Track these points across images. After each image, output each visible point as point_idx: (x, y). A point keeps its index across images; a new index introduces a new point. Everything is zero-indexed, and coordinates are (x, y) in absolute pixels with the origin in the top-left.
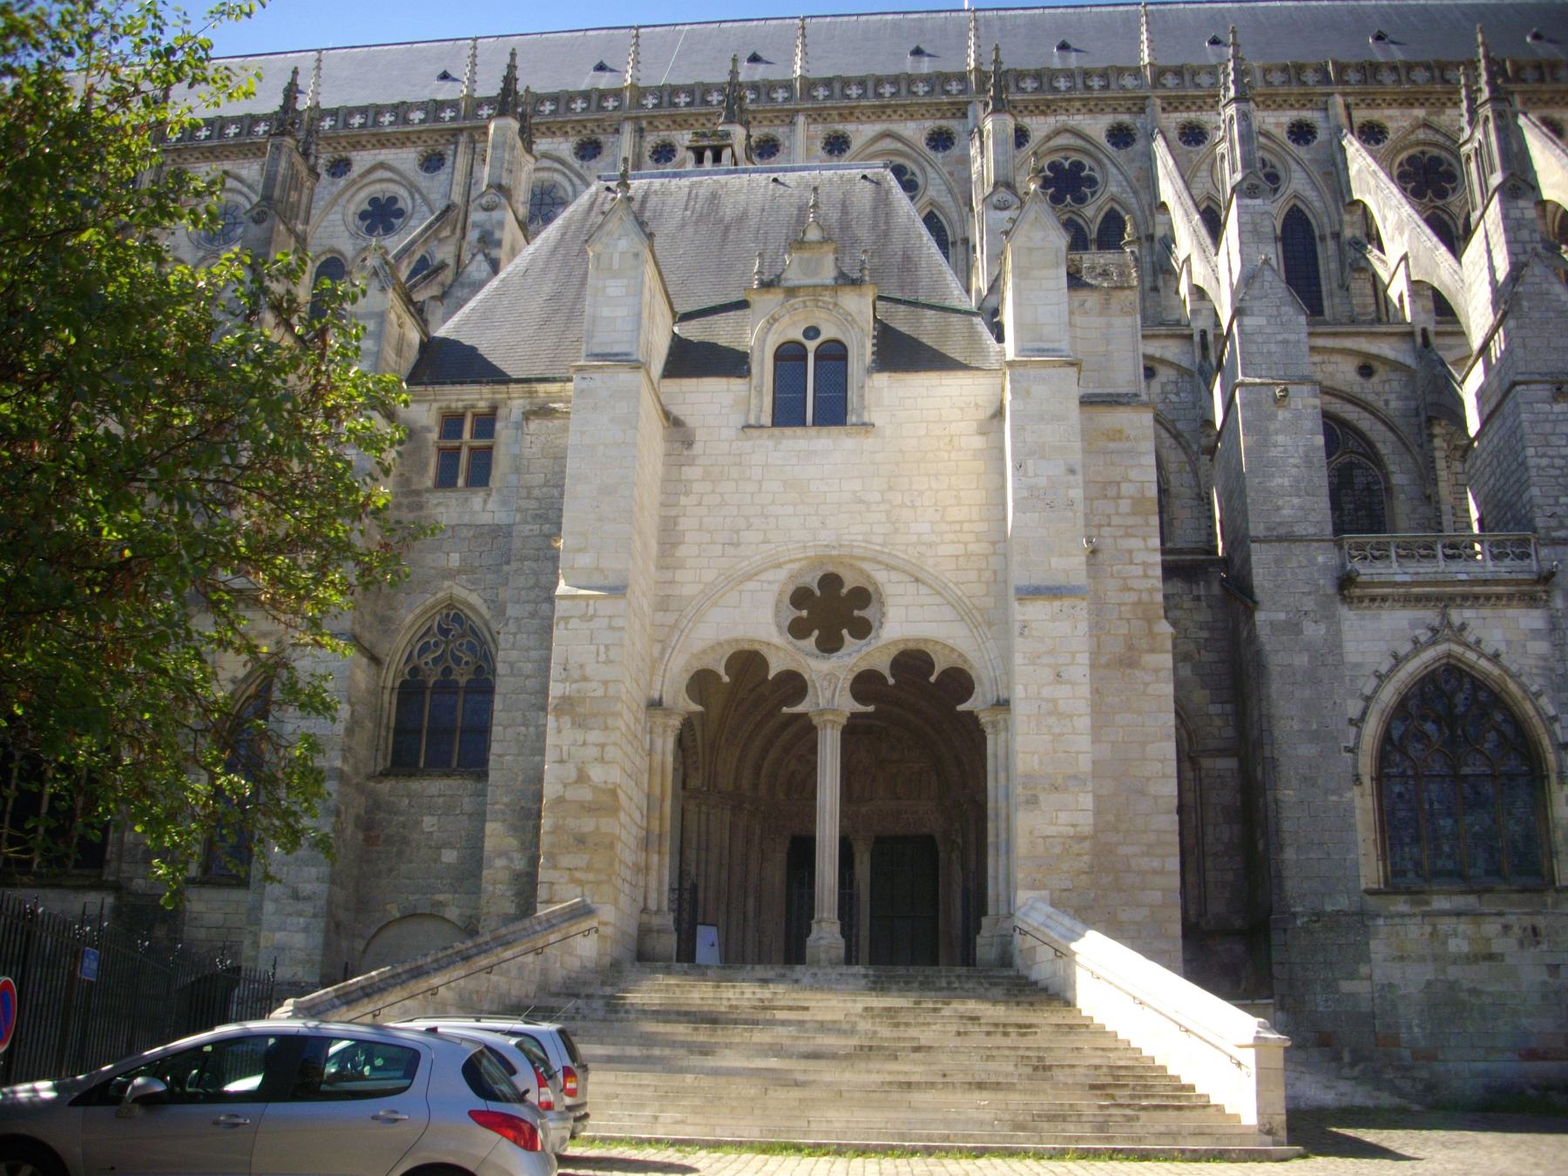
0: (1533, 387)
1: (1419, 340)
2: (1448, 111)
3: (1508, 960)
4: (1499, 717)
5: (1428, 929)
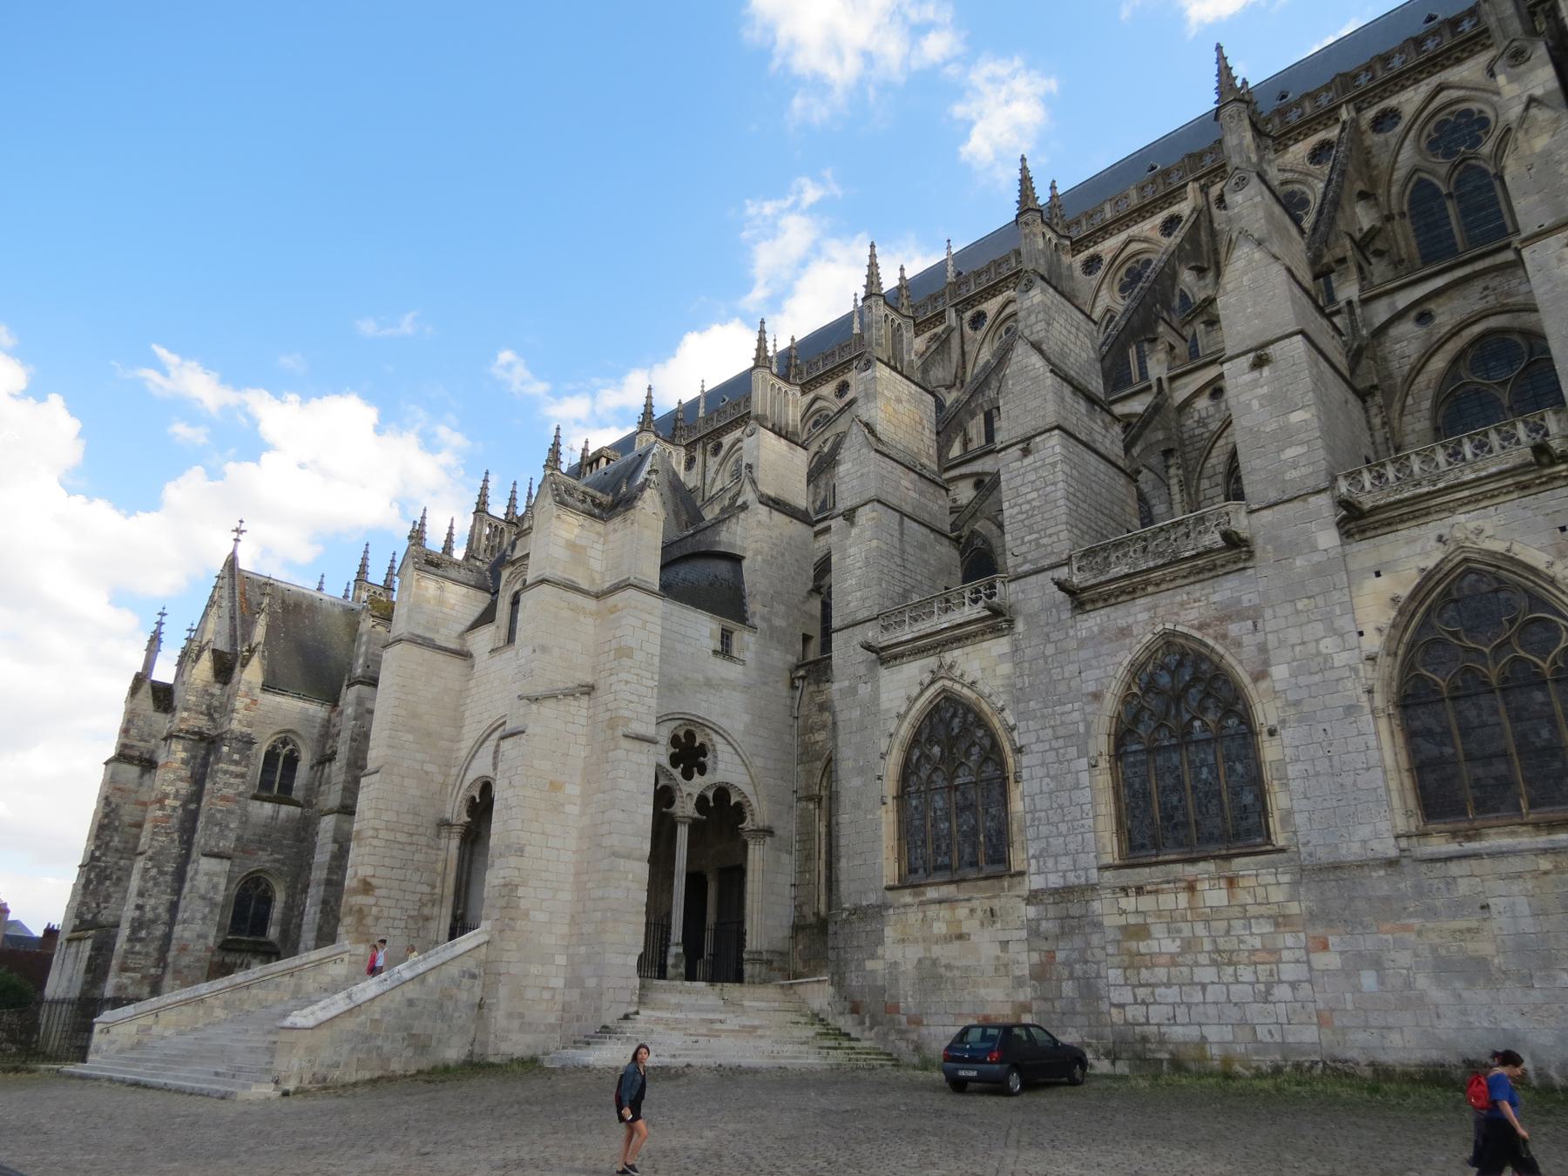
2: (1291, 149)
5: (920, 915)
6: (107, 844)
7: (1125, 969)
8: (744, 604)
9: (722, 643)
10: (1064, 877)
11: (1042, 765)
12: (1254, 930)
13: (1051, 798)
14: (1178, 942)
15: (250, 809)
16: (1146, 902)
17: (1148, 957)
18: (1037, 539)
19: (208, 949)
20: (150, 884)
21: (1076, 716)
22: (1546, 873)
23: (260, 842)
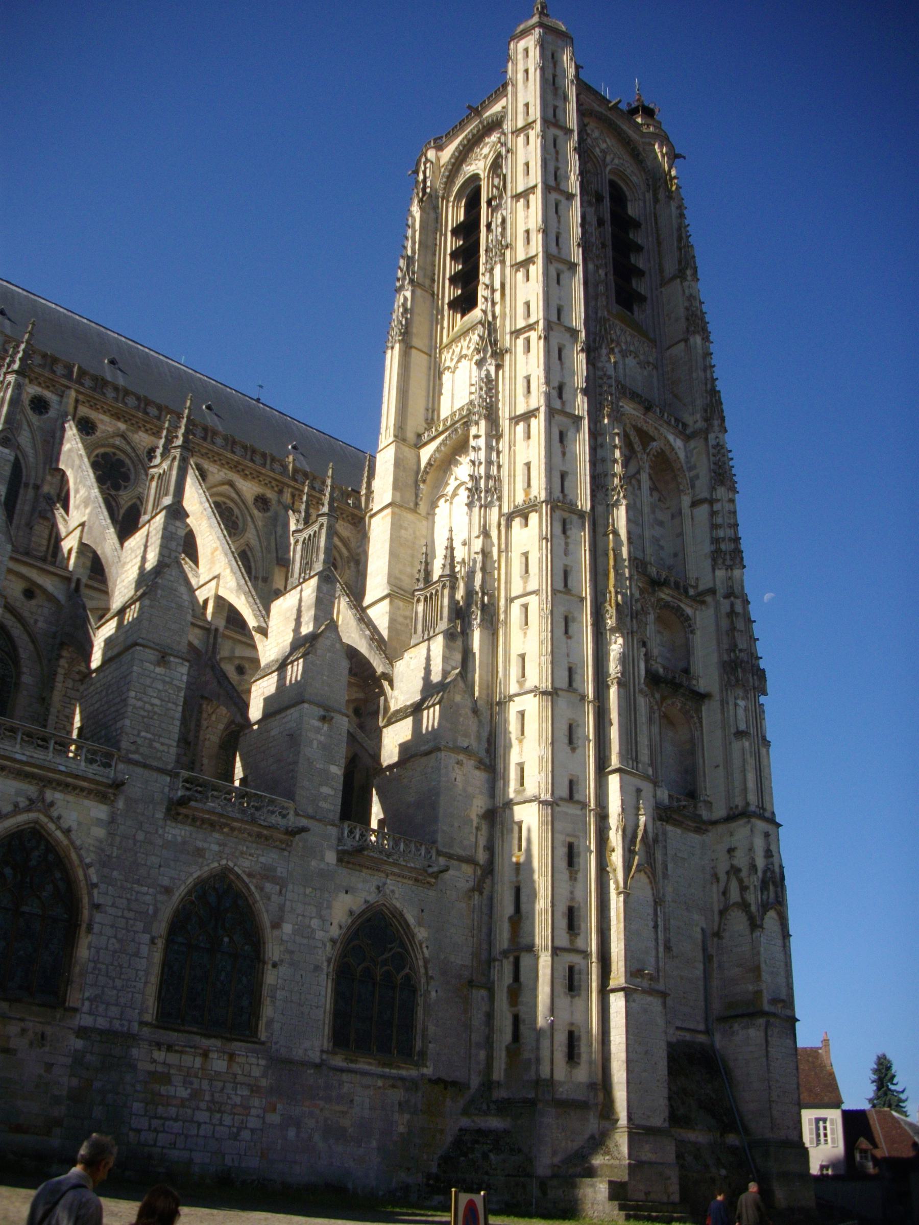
0: (147, 650)
1: (73, 585)
2: (141, 433)
4: (58, 875)
10: (111, 1022)
11: (112, 926)
12: (238, 1092)
14: (189, 1091)
16: (172, 1058)
18: (150, 739)
22: (379, 1088)
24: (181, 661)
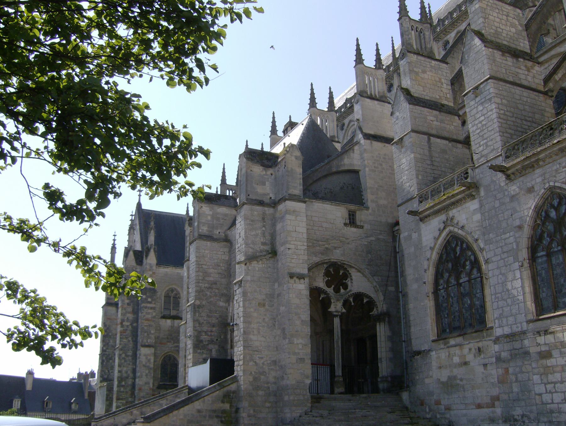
3: (472, 364)
6: (108, 344)
7: (541, 375)
8: (362, 195)
9: (350, 219)
10: (511, 328)
13: (503, 286)
15: (161, 323)
17: (551, 368)
18: (486, 143)
19: (150, 389)
20: (123, 361)
21: (512, 239)
23: (168, 338)
24: (486, 83)
